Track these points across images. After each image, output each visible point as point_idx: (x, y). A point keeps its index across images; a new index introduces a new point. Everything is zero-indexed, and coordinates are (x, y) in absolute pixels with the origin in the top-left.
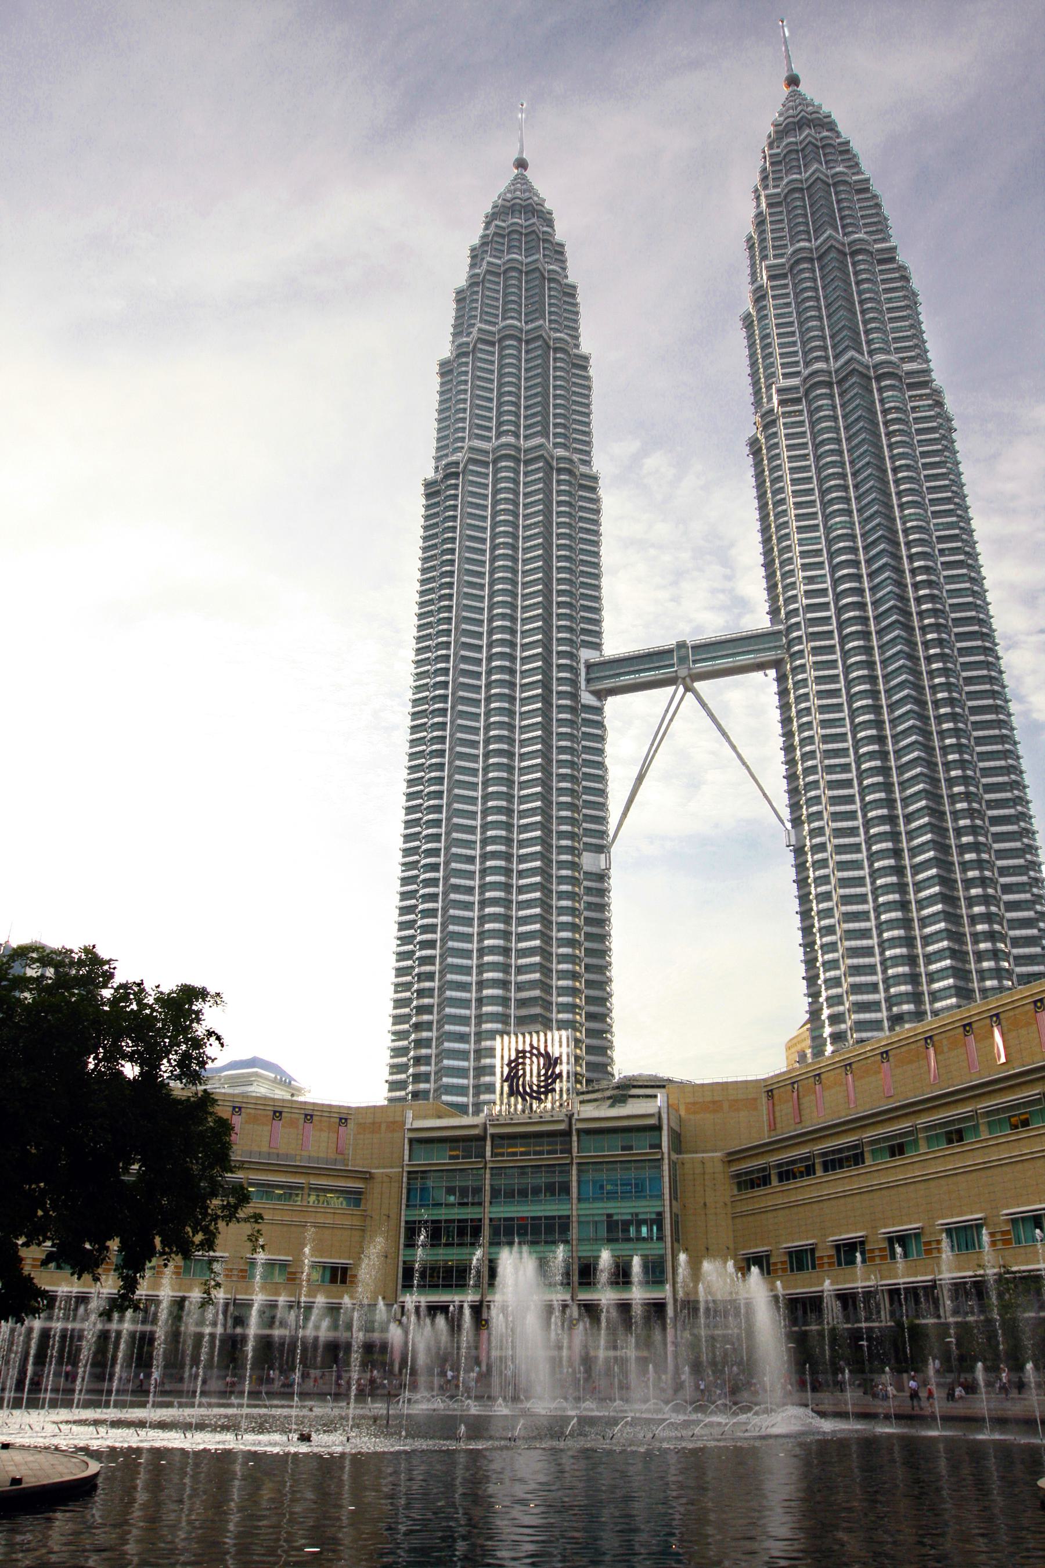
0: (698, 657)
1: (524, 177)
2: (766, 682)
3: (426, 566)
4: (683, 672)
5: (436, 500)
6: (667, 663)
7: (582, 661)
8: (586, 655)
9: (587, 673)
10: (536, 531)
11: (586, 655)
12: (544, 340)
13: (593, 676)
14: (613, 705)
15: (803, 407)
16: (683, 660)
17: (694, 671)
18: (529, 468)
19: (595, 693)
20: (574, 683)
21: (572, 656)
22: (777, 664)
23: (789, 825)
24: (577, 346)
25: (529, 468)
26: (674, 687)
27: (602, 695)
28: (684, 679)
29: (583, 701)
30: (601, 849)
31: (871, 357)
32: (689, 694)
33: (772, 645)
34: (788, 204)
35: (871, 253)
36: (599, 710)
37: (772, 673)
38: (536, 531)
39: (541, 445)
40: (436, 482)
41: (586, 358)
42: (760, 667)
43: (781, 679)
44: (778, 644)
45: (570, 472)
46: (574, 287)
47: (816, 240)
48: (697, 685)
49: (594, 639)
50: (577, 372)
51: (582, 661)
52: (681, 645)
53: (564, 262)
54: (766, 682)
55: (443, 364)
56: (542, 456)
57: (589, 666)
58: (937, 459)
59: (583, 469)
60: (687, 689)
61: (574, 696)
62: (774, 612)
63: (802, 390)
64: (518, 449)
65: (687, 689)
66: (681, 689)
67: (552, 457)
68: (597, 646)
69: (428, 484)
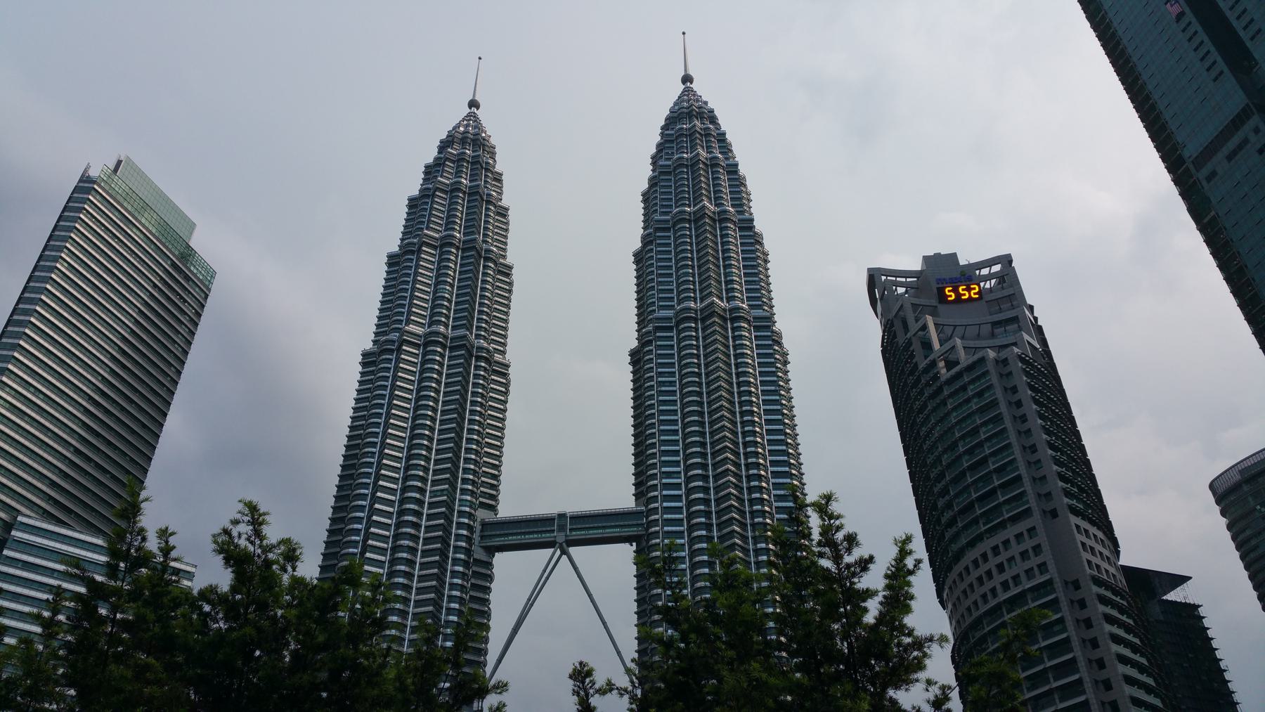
0: (574, 527)
1: (475, 116)
2: (626, 552)
3: (355, 424)
5: (371, 369)
6: (549, 529)
7: (479, 520)
8: (482, 514)
9: (482, 531)
10: (453, 407)
11: (482, 514)
12: (477, 251)
13: (486, 533)
14: (500, 559)
15: (674, 333)
16: (562, 528)
17: (570, 538)
18: (453, 354)
20: (469, 539)
21: (470, 516)
24: (504, 257)
25: (453, 354)
26: (549, 551)
27: (491, 551)
28: (561, 544)
29: (475, 556)
31: (728, 302)
32: (564, 557)
33: (635, 522)
34: (676, 175)
35: (735, 222)
36: (489, 565)
38: (453, 407)
39: (465, 336)
40: (374, 353)
44: (639, 522)
45: (487, 360)
46: (507, 209)
47: (694, 206)
48: (573, 550)
50: (501, 277)
51: (479, 520)
52: (562, 516)
53: (501, 188)
54: (626, 552)
55: (391, 257)
56: (465, 345)
57: (484, 525)
58: (773, 388)
59: (498, 357)
60: (564, 552)
61: (468, 552)
62: (638, 496)
63: (674, 320)
64: (445, 337)
65: (564, 552)
66: (558, 552)
67: (473, 347)
68: (493, 508)
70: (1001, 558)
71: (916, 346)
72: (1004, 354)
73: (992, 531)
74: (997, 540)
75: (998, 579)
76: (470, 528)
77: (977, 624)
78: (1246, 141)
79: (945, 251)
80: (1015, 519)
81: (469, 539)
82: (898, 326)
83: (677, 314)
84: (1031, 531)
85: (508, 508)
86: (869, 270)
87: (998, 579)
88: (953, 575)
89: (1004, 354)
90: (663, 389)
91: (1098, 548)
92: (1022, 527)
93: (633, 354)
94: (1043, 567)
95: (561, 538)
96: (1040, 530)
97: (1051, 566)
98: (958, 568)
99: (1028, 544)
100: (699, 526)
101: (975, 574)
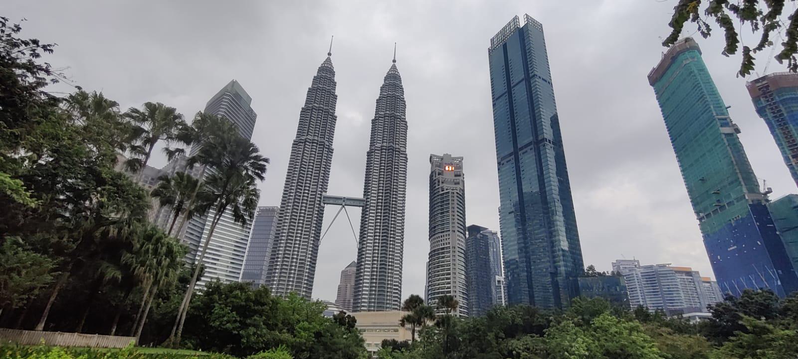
4: (344, 204)
16: (344, 201)
19: (324, 203)
20: (320, 201)
22: (363, 206)
27: (324, 203)
36: (324, 207)
37: (361, 208)
41: (336, 117)
42: (360, 206)
43: (363, 210)
48: (346, 207)
49: (324, 187)
52: (344, 198)
57: (324, 197)
60: (343, 207)
61: (320, 204)
62: (364, 195)
64: (318, 141)
68: (326, 192)
70: (442, 238)
71: (436, 181)
72: (453, 191)
73: (442, 232)
74: (442, 234)
75: (441, 243)
76: (320, 198)
77: (435, 251)
78: (510, 160)
79: (449, 154)
80: (447, 231)
81: (320, 201)
82: (434, 174)
83: (382, 146)
85: (331, 191)
89: (453, 191)
91: (461, 239)
92: (447, 233)
93: (368, 153)
94: (449, 243)
95: (344, 204)
98: (434, 237)
99: (448, 237)
100: (378, 216)
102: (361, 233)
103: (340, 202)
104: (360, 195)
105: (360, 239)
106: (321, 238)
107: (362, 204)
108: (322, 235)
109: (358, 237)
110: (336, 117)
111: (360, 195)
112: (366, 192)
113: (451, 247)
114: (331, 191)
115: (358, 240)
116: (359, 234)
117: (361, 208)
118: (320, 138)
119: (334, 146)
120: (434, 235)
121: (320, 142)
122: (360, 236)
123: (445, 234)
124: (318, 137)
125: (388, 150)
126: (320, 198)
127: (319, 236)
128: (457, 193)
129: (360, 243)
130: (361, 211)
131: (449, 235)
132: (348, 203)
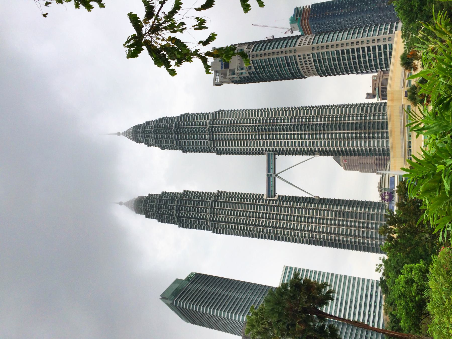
4: (274, 175)
8: (265, 197)
10: (234, 205)
11: (265, 197)
16: (271, 175)
20: (273, 200)
22: (275, 155)
23: (314, 156)
30: (313, 199)
36: (279, 196)
37: (277, 156)
41: (185, 191)
42: (275, 159)
43: (279, 154)
45: (218, 197)
48: (276, 173)
52: (267, 175)
57: (268, 196)
60: (277, 175)
61: (276, 200)
62: (263, 154)
68: (263, 195)
69: (214, 232)
73: (297, 65)
74: (299, 64)
77: (317, 71)
82: (234, 80)
83: (210, 140)
84: (299, 56)
86: (213, 85)
87: (309, 65)
88: (303, 73)
90: (233, 145)
93: (218, 154)
94: (308, 55)
95: (274, 175)
96: (299, 54)
97: (308, 53)
101: (306, 70)
102: (303, 154)
103: (272, 179)
104: (263, 158)
105: (310, 155)
106: (311, 196)
107: (273, 156)
108: (308, 196)
109: (308, 157)
110: (185, 191)
111: (263, 158)
112: (260, 153)
113: (313, 52)
114: (262, 190)
115: (311, 156)
116: (304, 156)
117: (277, 156)
118: (208, 206)
119: (214, 190)
120: (300, 72)
121: (212, 206)
122: (307, 154)
123: (298, 61)
124: (207, 208)
125: (213, 132)
126: (270, 200)
127: (310, 198)
128: (253, 51)
129: (314, 154)
130: (280, 156)
131: (299, 56)
132: (272, 171)
